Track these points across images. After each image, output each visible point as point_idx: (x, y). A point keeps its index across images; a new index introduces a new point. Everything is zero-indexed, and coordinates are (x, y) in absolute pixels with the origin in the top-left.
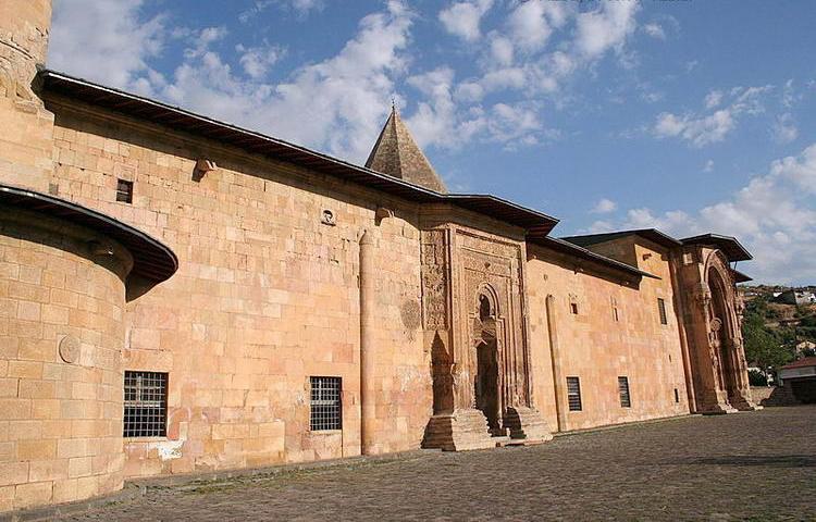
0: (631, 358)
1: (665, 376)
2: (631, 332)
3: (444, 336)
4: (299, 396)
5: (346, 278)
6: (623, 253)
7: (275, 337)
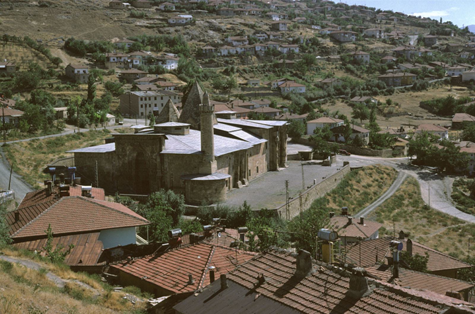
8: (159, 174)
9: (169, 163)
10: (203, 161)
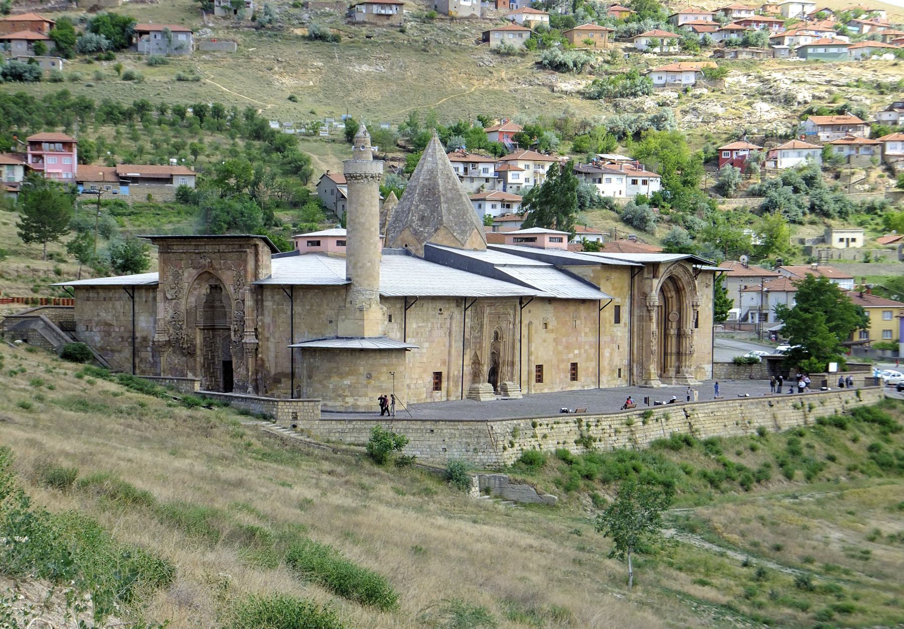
0: (583, 351)
1: (611, 360)
2: (586, 334)
3: (478, 353)
4: (429, 379)
5: (445, 333)
7: (425, 360)
8: (250, 339)
9: (274, 309)
10: (348, 305)
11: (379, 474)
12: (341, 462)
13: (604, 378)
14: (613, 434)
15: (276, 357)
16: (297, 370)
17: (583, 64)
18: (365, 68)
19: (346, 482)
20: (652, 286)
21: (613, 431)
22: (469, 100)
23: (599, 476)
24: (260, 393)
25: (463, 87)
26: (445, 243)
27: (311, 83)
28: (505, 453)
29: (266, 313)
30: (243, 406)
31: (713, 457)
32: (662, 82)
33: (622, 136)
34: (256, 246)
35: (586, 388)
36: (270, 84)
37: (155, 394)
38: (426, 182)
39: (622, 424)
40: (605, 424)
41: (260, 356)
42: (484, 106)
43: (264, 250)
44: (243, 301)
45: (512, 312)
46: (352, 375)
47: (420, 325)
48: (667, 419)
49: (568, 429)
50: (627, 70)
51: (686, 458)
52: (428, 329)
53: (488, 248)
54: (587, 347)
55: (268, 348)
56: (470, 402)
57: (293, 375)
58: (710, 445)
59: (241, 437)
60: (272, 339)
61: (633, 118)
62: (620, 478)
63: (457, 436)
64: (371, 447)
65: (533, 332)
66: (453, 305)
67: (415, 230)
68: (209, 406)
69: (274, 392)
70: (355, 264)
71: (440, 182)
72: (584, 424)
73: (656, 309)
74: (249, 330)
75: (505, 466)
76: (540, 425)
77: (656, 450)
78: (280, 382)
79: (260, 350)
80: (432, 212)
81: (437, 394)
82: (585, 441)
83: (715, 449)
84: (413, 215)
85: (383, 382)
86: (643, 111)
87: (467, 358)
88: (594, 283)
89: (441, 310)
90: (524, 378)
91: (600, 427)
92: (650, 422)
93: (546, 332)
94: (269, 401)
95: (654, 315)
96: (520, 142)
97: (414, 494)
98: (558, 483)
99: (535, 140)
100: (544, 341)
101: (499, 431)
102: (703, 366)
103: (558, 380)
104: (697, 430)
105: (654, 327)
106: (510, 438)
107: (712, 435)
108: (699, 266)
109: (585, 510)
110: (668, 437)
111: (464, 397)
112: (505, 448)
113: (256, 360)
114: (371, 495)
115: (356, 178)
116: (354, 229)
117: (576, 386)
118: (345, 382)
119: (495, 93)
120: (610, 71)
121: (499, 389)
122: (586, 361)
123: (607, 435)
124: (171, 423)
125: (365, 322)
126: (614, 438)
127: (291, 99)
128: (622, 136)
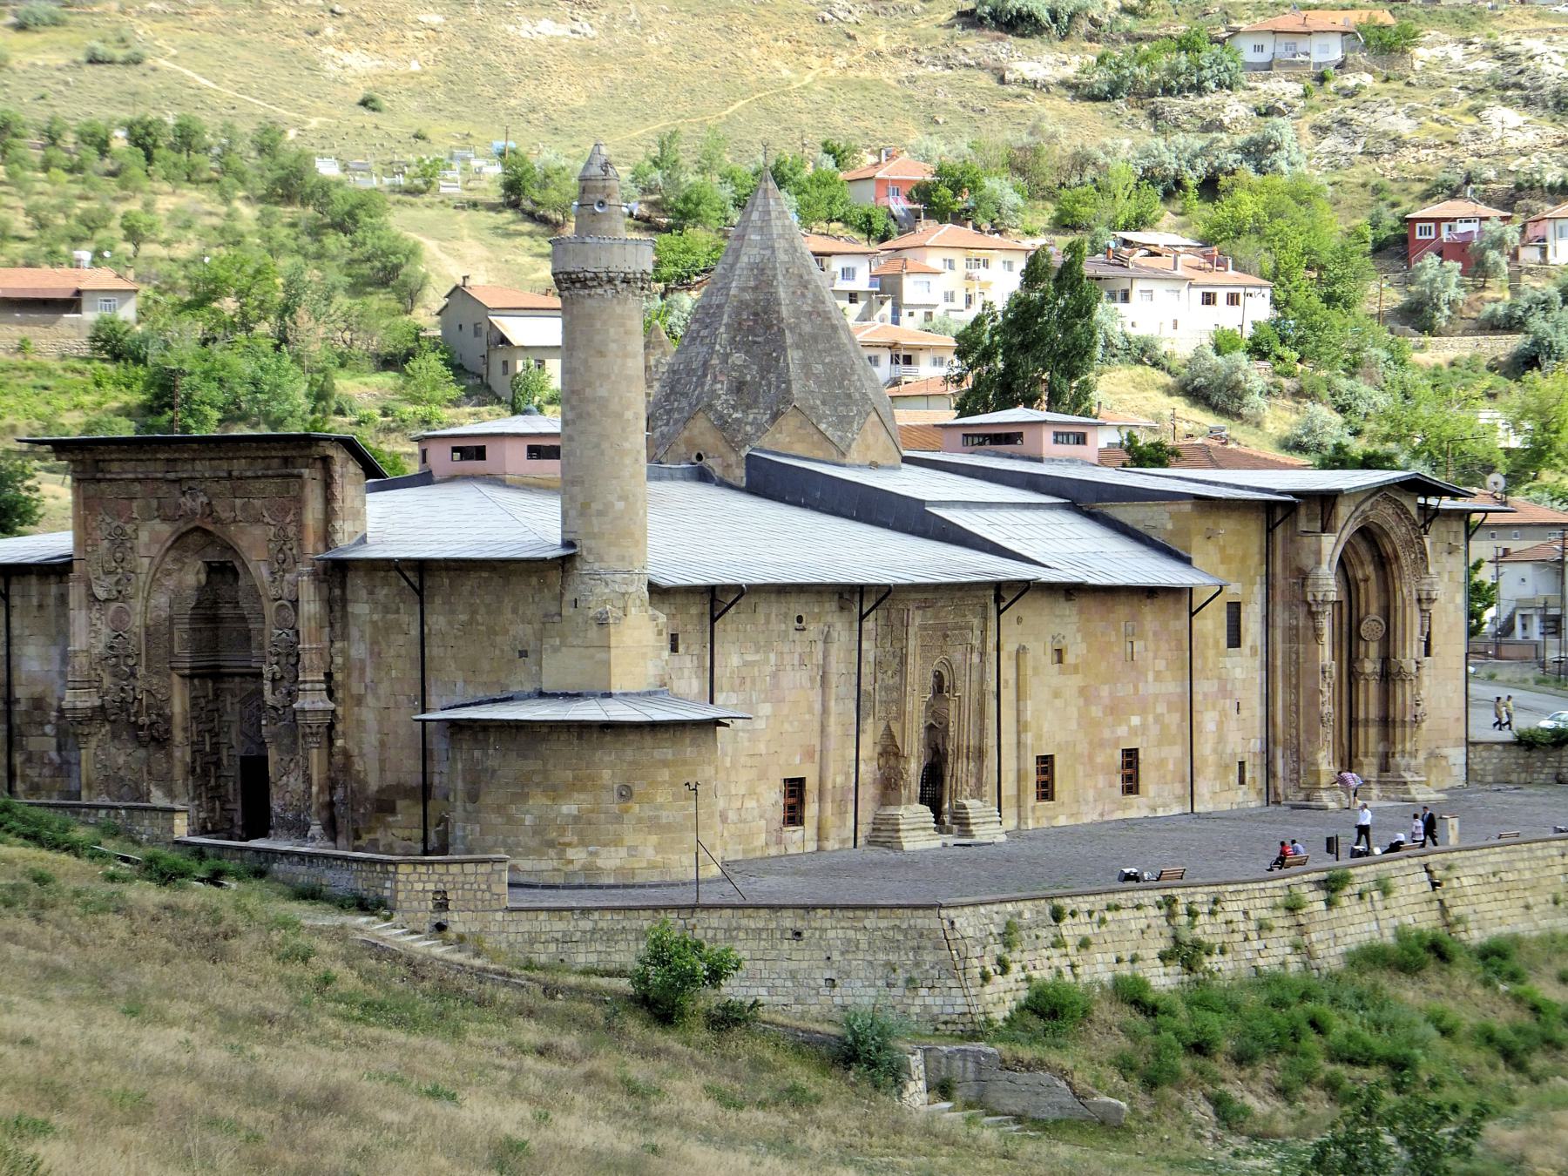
0: (1151, 718)
1: (1221, 739)
2: (1158, 675)
3: (896, 728)
4: (773, 798)
5: (812, 679)
6: (1170, 526)
7: (762, 748)
8: (312, 701)
9: (374, 624)
10: (568, 611)
11: (667, 1051)
12: (568, 1021)
13: (1203, 787)
14: (1252, 935)
15: (382, 744)
16: (436, 780)
17: (1071, 17)
18: (547, 28)
19: (590, 1077)
20: (1318, 552)
21: (1253, 925)
22: (800, 104)
23: (1227, 1045)
24: (341, 841)
25: (786, 73)
26: (799, 449)
27: (415, 67)
28: (988, 988)
29: (354, 632)
30: (304, 875)
31: (1503, 988)
32: (1263, 57)
33: (1173, 189)
34: (326, 461)
35: (1160, 813)
36: (313, 68)
37: (72, 848)
38: (747, 296)
39: (1275, 907)
40: (1232, 908)
41: (339, 743)
42: (837, 119)
43: (346, 471)
44: (295, 603)
45: (976, 622)
46: (583, 789)
47: (749, 658)
48: (1386, 891)
49: (1143, 924)
50: (1180, 29)
51: (1439, 994)
52: (768, 669)
53: (906, 460)
54: (1161, 708)
55: (360, 723)
56: (876, 854)
57: (425, 792)
58: (1494, 956)
59: (305, 959)
60: (370, 700)
61: (1198, 143)
62: (1279, 1050)
63: (864, 945)
64: (643, 979)
65: (1029, 672)
66: (831, 606)
67: (721, 417)
68: (215, 878)
69: (379, 834)
70: (585, 506)
71: (782, 294)
72: (1181, 908)
73: (1329, 608)
74: (312, 676)
75: (989, 1022)
76: (1073, 914)
77: (1361, 974)
78: (392, 810)
79: (339, 727)
80: (764, 371)
81: (794, 834)
82: (1184, 953)
83: (1508, 966)
84: (715, 381)
85: (661, 807)
86: (1221, 127)
87: (867, 740)
88: (1175, 545)
89: (800, 619)
90: (1009, 789)
91: (1221, 918)
92: (1344, 901)
93: (1061, 673)
94: (373, 862)
95: (1326, 625)
96: (930, 203)
97: (762, 1105)
98: (1125, 1066)
99: (965, 200)
100: (1056, 695)
101: (970, 932)
102: (1445, 752)
103: (1091, 794)
104: (1459, 920)
105: (1325, 654)
106: (999, 950)
107: (1495, 931)
108: (1432, 501)
109: (1199, 1137)
110: (1389, 939)
111: (861, 841)
112: (985, 977)
113: (331, 755)
114: (656, 1110)
115: (584, 283)
116: (580, 416)
117: (1136, 808)
118: (565, 809)
119: (863, 86)
120: (1137, 31)
121: (947, 818)
122: (1160, 744)
123: (1238, 937)
124: (118, 926)
125: (613, 652)
126: (1257, 945)
127: (364, 103)
128: (1173, 189)
